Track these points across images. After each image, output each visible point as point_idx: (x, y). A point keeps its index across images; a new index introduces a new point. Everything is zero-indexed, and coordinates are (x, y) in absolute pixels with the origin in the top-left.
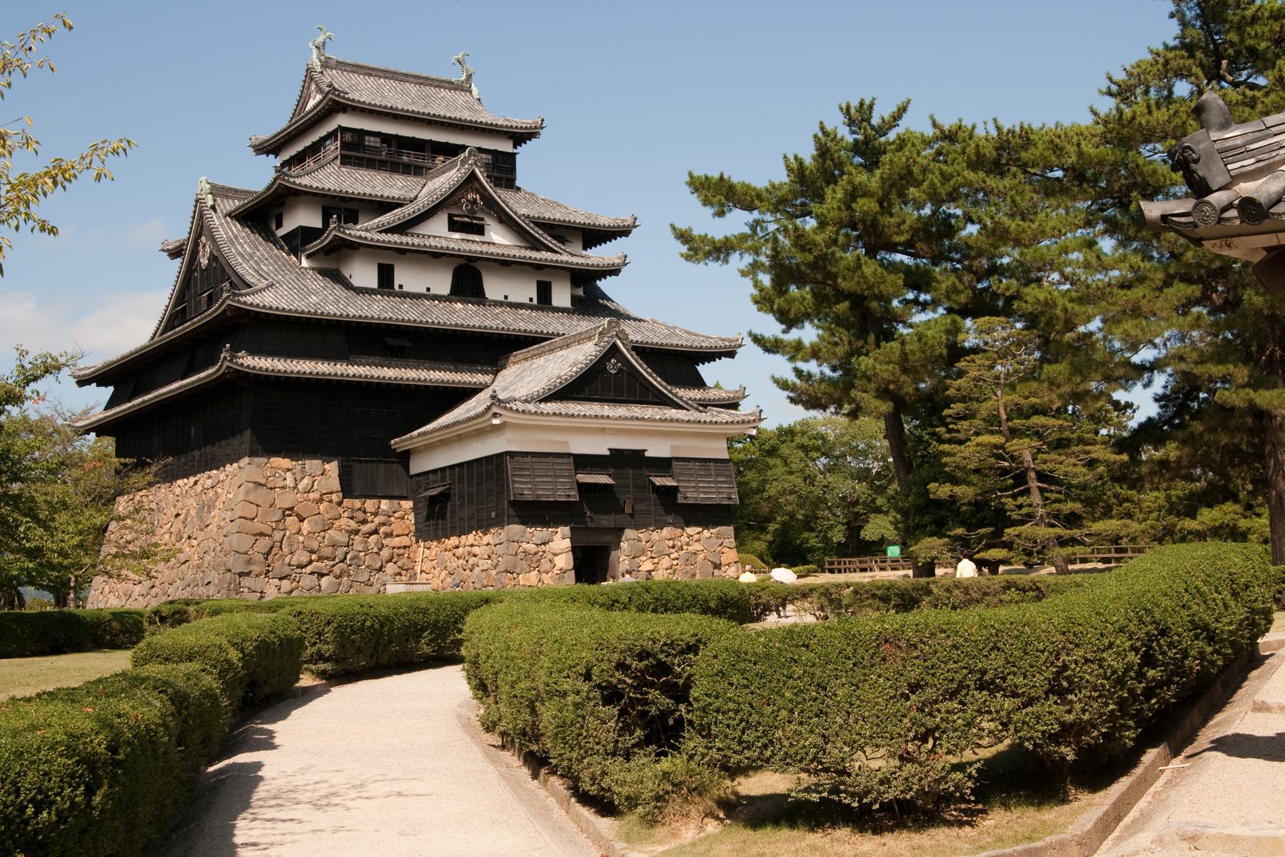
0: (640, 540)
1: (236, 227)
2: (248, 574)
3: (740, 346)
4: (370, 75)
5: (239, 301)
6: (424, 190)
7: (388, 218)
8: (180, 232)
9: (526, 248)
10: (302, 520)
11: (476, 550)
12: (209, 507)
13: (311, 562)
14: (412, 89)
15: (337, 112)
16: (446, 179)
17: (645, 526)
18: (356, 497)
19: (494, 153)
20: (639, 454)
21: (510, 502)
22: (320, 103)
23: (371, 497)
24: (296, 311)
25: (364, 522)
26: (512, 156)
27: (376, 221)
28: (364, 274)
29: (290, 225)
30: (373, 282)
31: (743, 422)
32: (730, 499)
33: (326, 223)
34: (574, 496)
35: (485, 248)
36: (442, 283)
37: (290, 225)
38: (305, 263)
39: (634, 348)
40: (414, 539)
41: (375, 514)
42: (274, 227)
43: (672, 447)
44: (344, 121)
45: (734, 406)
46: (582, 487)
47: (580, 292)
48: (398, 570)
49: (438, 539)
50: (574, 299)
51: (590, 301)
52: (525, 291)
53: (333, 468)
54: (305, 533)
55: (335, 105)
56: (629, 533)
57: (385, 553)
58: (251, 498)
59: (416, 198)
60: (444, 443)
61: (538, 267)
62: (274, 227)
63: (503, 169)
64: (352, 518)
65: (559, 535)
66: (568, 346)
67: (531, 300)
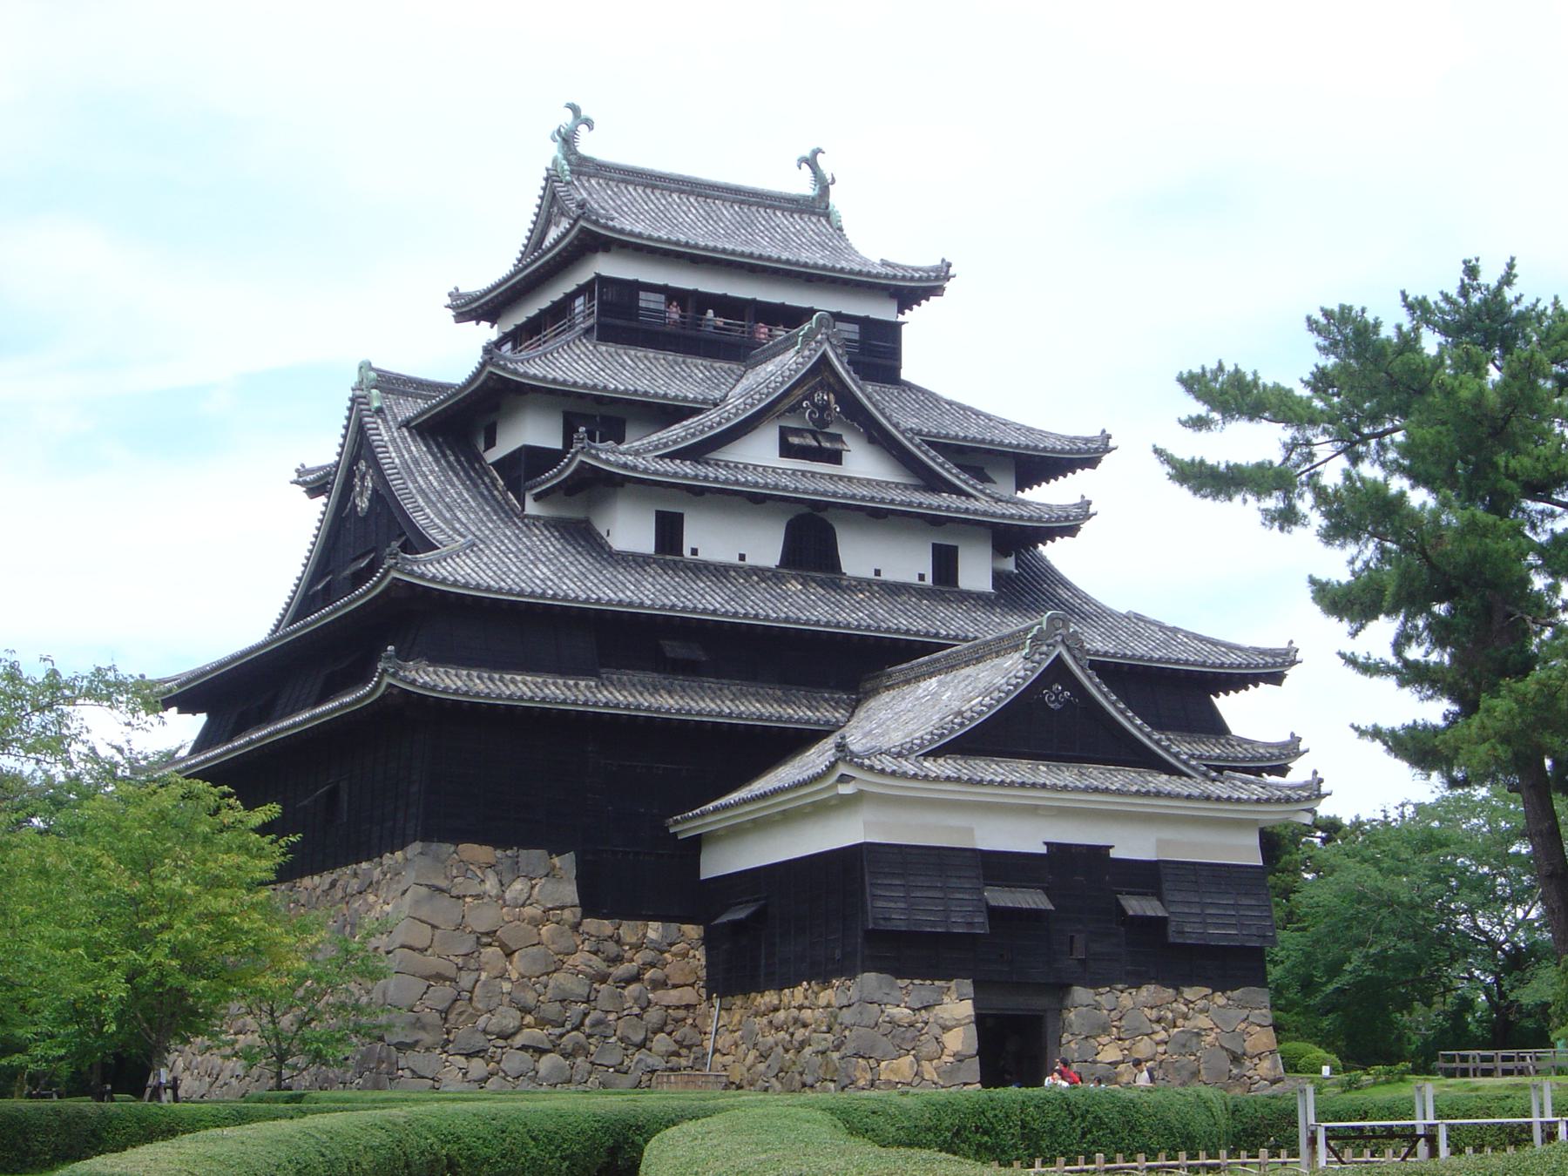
0: (1098, 1007)
1: (417, 449)
2: (412, 1046)
3: (1293, 663)
4: (654, 187)
5: (411, 573)
6: (739, 389)
7: (677, 433)
8: (326, 450)
9: (916, 488)
10: (509, 954)
11: (807, 1014)
12: (353, 925)
14: (727, 212)
15: (596, 251)
16: (779, 368)
19: (865, 323)
22: (564, 235)
24: (510, 592)
25: (617, 960)
26: (892, 332)
27: (654, 437)
28: (631, 530)
29: (506, 445)
31: (1288, 800)
33: (568, 441)
34: (981, 924)
35: (841, 488)
36: (764, 545)
37: (506, 445)
38: (532, 508)
39: (1092, 665)
40: (703, 992)
41: (637, 947)
42: (481, 447)
43: (1161, 844)
44: (607, 266)
45: (1282, 771)
47: (1009, 564)
48: (675, 1047)
49: (745, 992)
50: (999, 578)
51: (1027, 585)
52: (909, 562)
53: (566, 863)
54: (514, 976)
55: (590, 242)
56: (1081, 994)
57: (654, 1015)
58: (424, 913)
59: (724, 399)
60: (760, 825)
61: (935, 521)
62: (481, 447)
63: (878, 351)
64: (595, 953)
66: (978, 660)
67: (922, 577)
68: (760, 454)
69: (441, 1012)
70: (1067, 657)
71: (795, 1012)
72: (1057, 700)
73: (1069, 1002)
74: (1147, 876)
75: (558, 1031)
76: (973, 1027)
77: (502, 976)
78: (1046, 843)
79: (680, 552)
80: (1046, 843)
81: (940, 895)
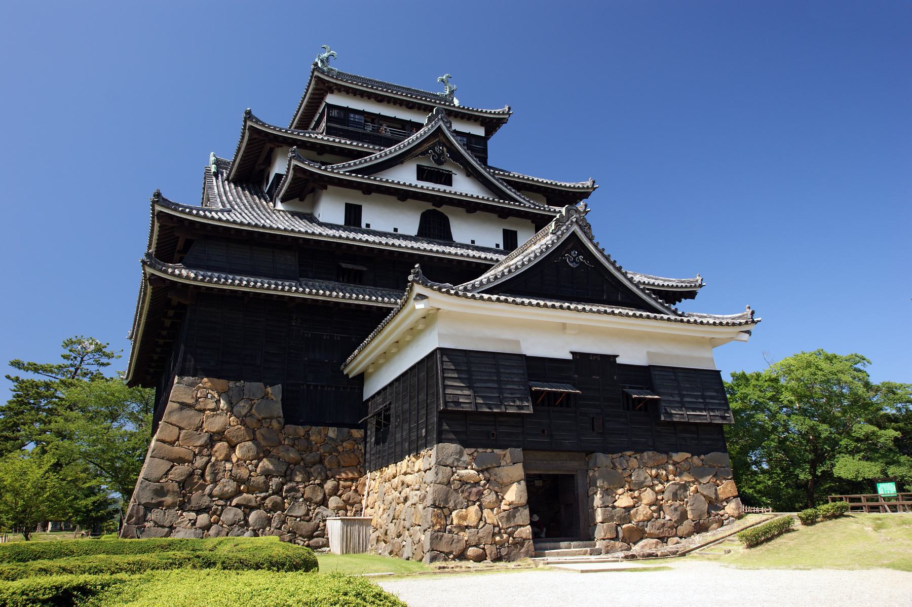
11: (409, 479)
13: (238, 493)
17: (620, 450)
18: (301, 424)
19: (468, 135)
20: (610, 359)
21: (440, 412)
23: (317, 425)
26: (483, 141)
30: (341, 222)
31: (734, 324)
32: (724, 418)
38: (280, 206)
43: (649, 354)
44: (332, 99)
46: (535, 396)
48: (341, 504)
53: (275, 392)
54: (234, 459)
65: (508, 459)
67: (498, 246)
68: (405, 176)
69: (179, 483)
70: (580, 234)
71: (402, 477)
72: (574, 261)
73: (591, 464)
74: (644, 375)
75: (263, 495)
76: (523, 482)
77: (228, 459)
78: (572, 353)
79: (360, 225)
80: (572, 353)
81: (495, 385)
